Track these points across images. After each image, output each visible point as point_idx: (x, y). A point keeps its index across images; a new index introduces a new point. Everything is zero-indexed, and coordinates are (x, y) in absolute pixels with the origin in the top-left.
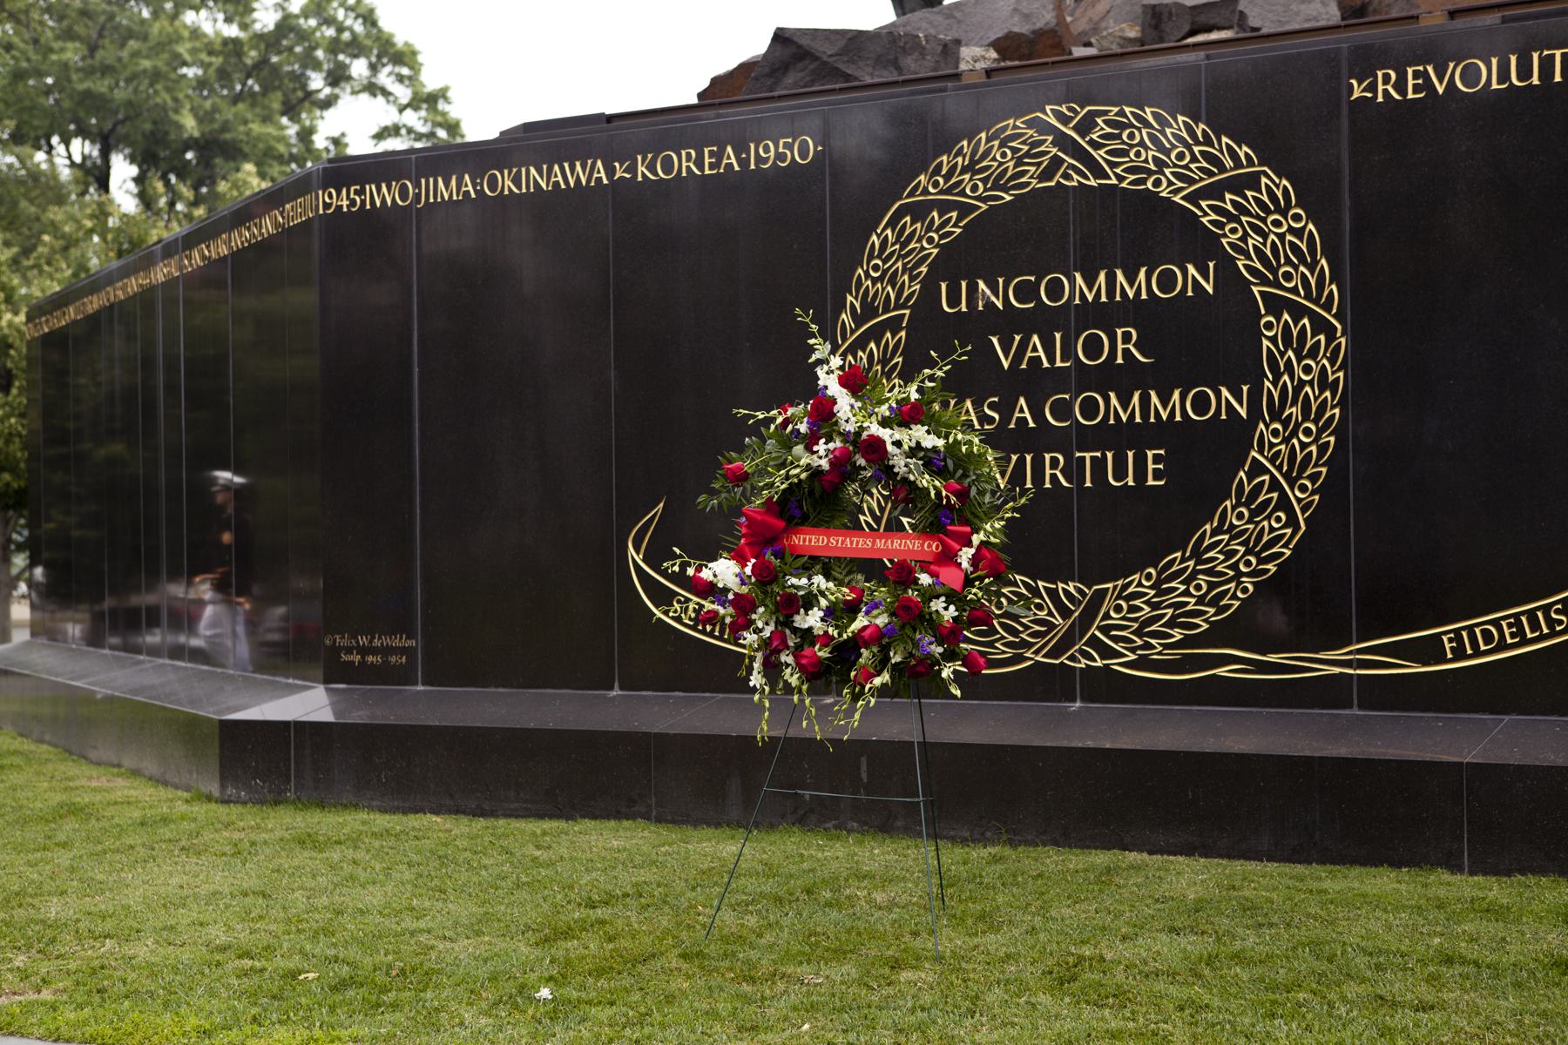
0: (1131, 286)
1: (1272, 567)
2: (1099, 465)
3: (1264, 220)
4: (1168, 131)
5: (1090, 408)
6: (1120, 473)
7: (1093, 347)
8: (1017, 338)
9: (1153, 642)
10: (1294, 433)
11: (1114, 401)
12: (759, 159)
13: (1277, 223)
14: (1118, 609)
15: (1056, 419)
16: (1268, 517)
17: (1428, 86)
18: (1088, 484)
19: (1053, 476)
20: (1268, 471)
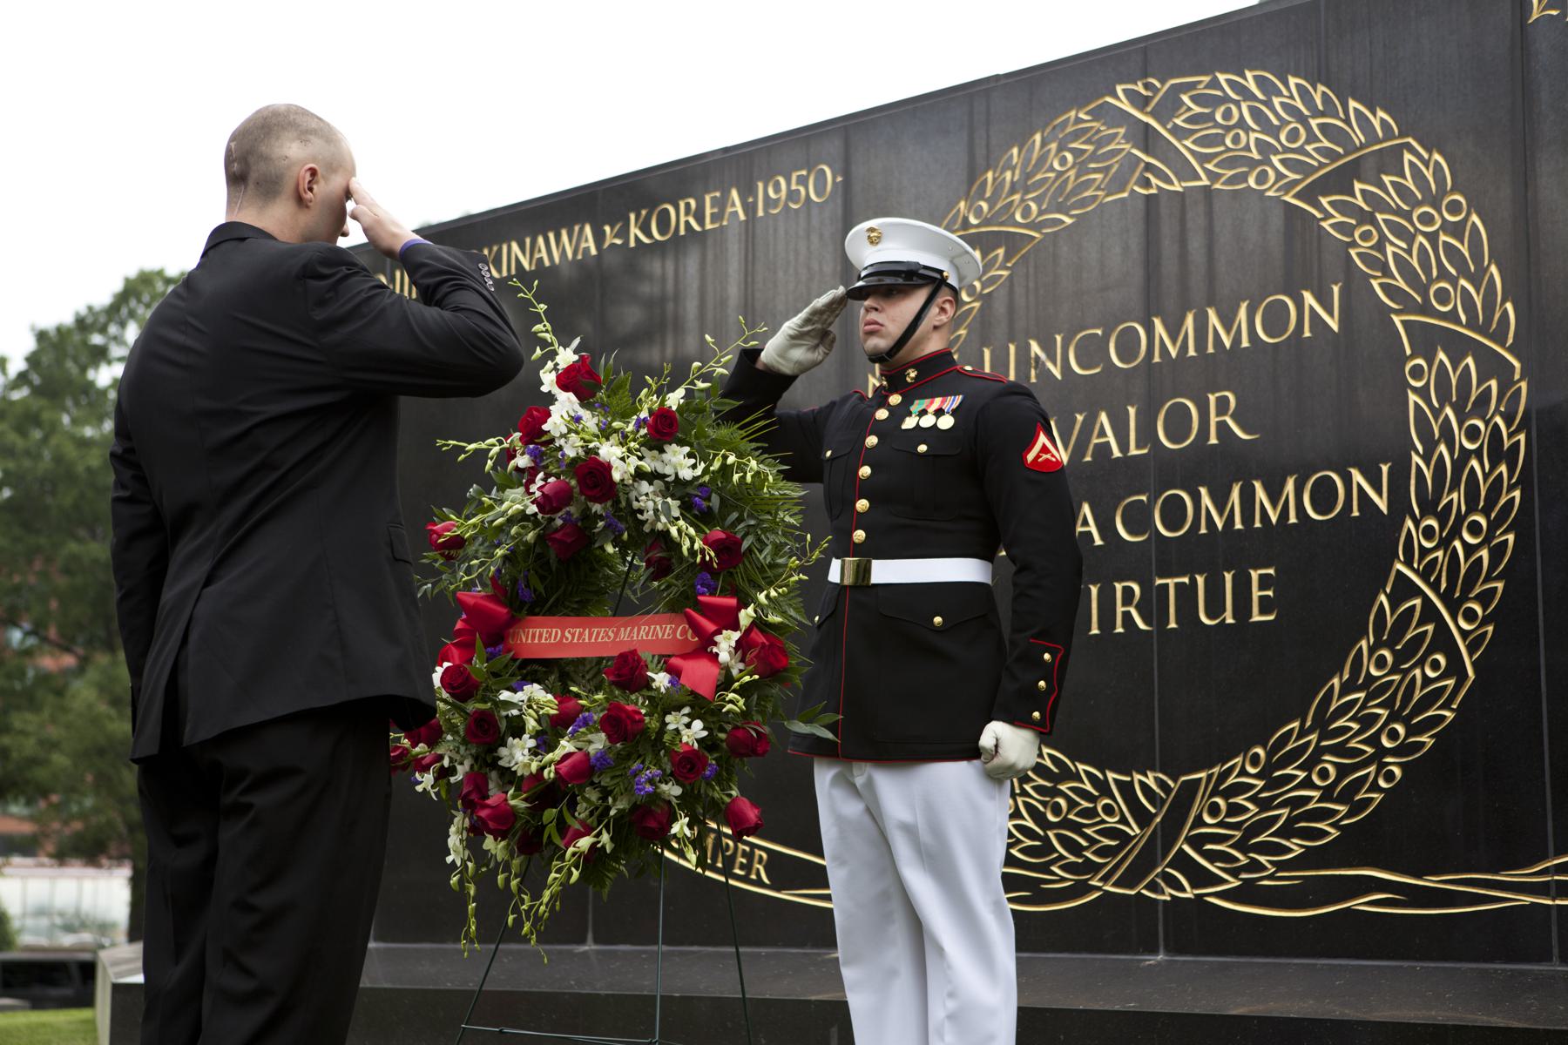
0: (1228, 331)
3: (1408, 216)
4: (1276, 101)
5: (1174, 513)
6: (1215, 608)
8: (1080, 418)
9: (1262, 859)
10: (1456, 533)
11: (1206, 500)
12: (769, 202)
13: (1427, 219)
14: (1214, 810)
15: (1130, 532)
16: (1421, 663)
18: (1173, 625)
19: (1127, 616)
20: (1420, 592)
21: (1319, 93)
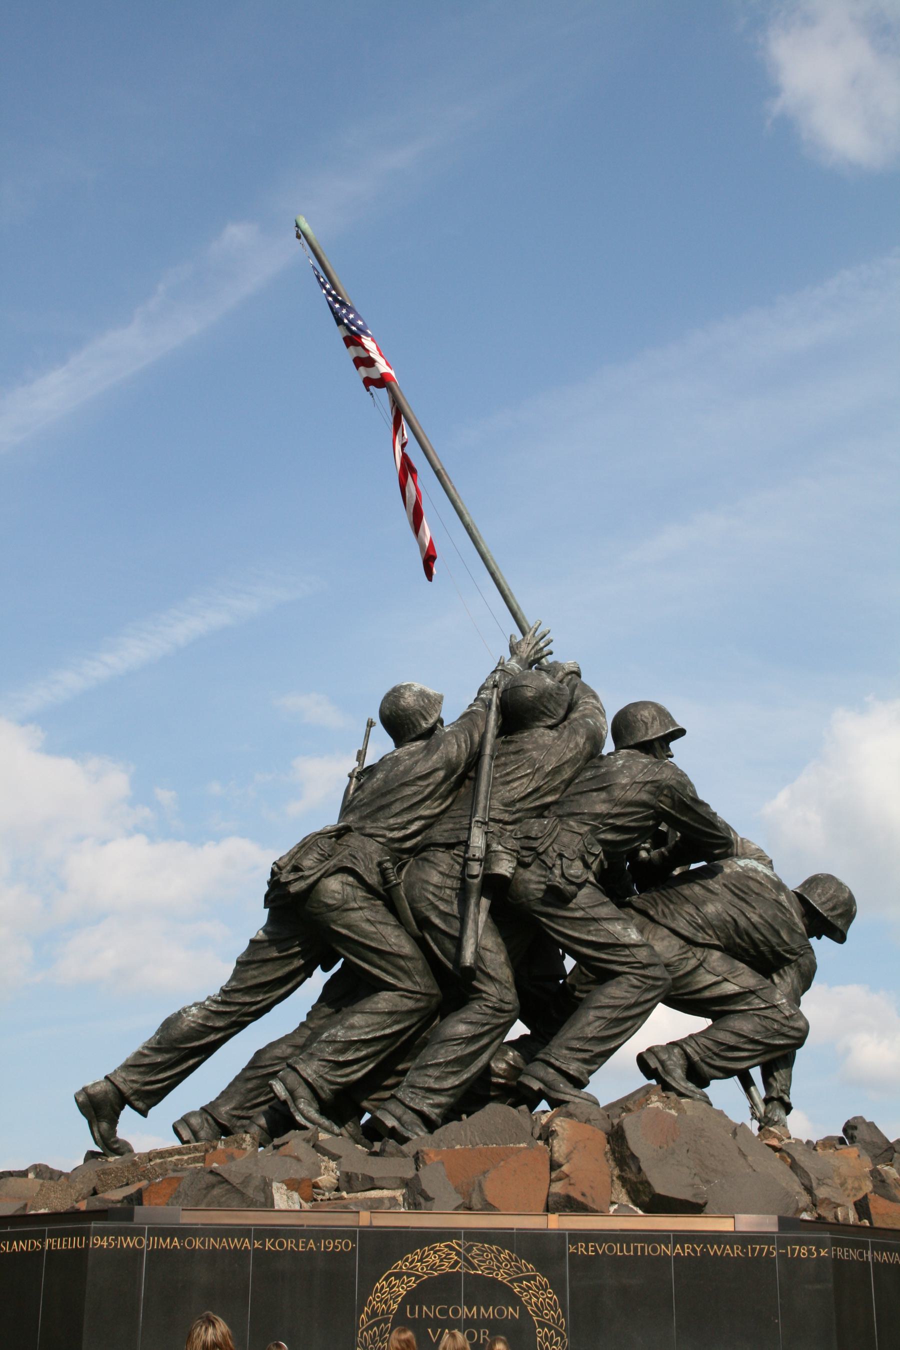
12: (325, 1247)
13: (542, 1294)
17: (596, 1251)
21: (514, 1256)
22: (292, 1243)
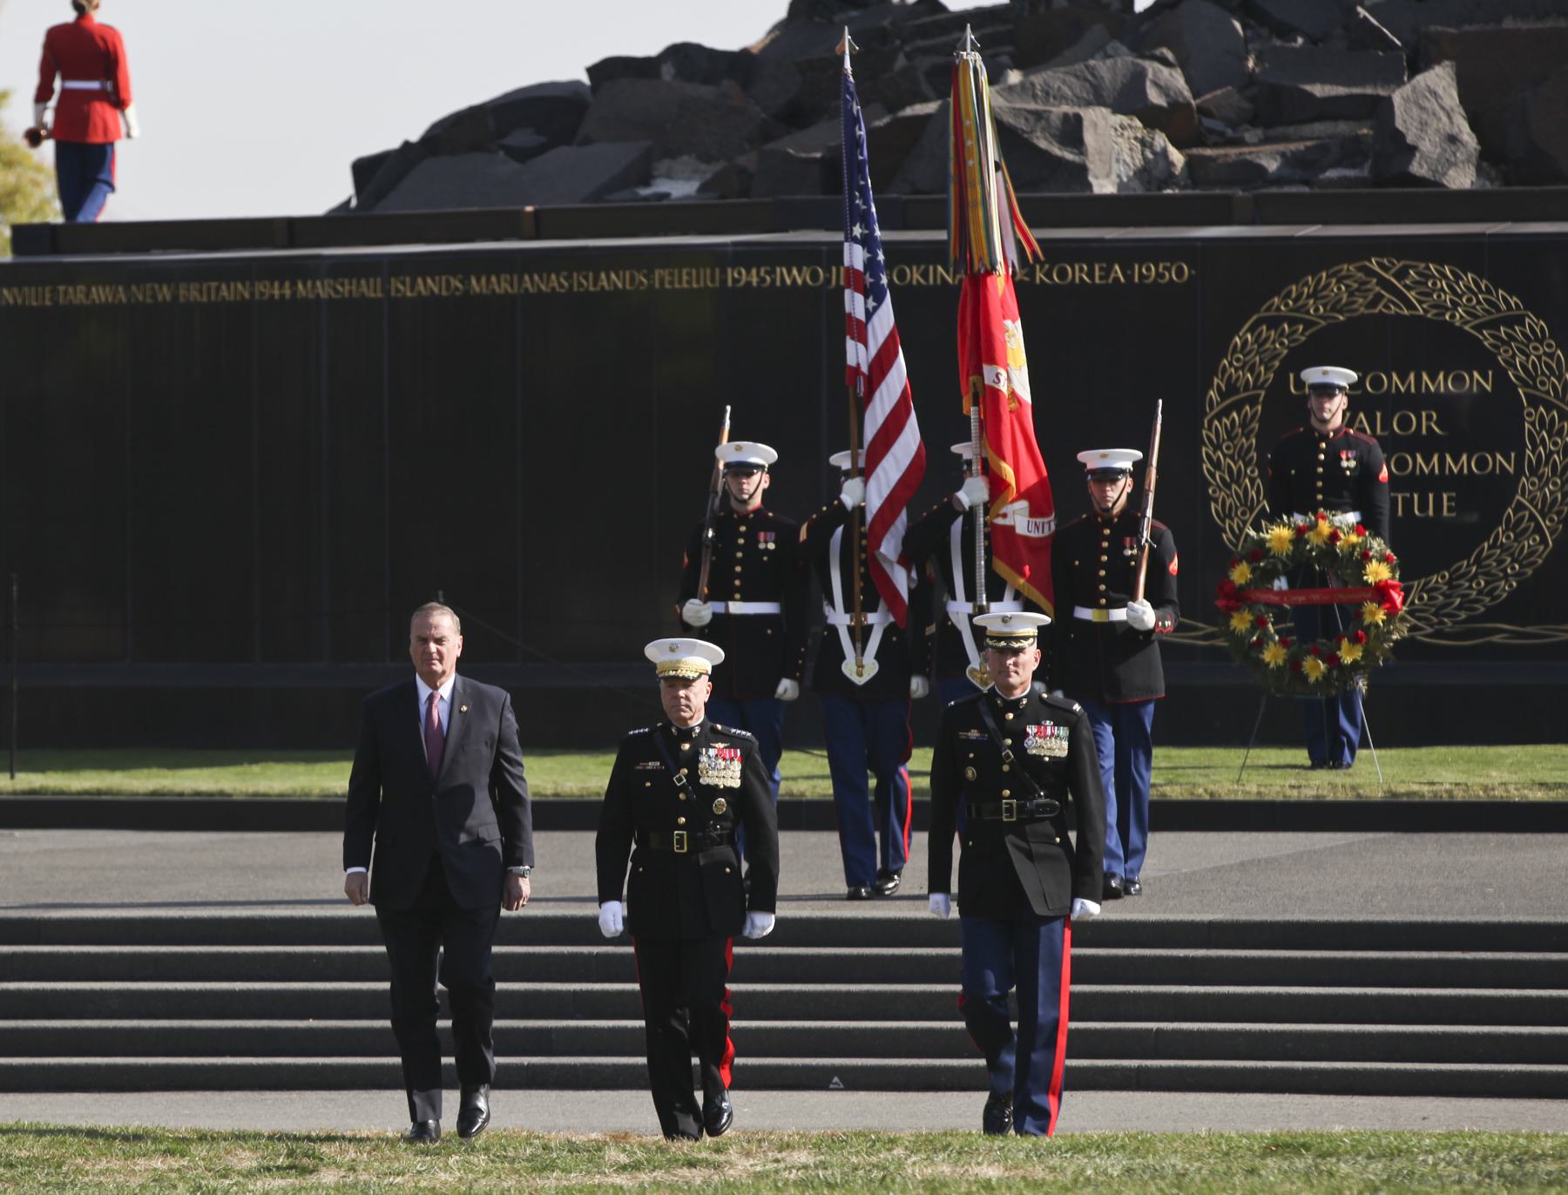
1: (1530, 572)
2: (1408, 503)
6: (1423, 506)
7: (1405, 422)
10: (1546, 484)
11: (1419, 459)
13: (1536, 349)
20: (1526, 508)
22: (1081, 270)
